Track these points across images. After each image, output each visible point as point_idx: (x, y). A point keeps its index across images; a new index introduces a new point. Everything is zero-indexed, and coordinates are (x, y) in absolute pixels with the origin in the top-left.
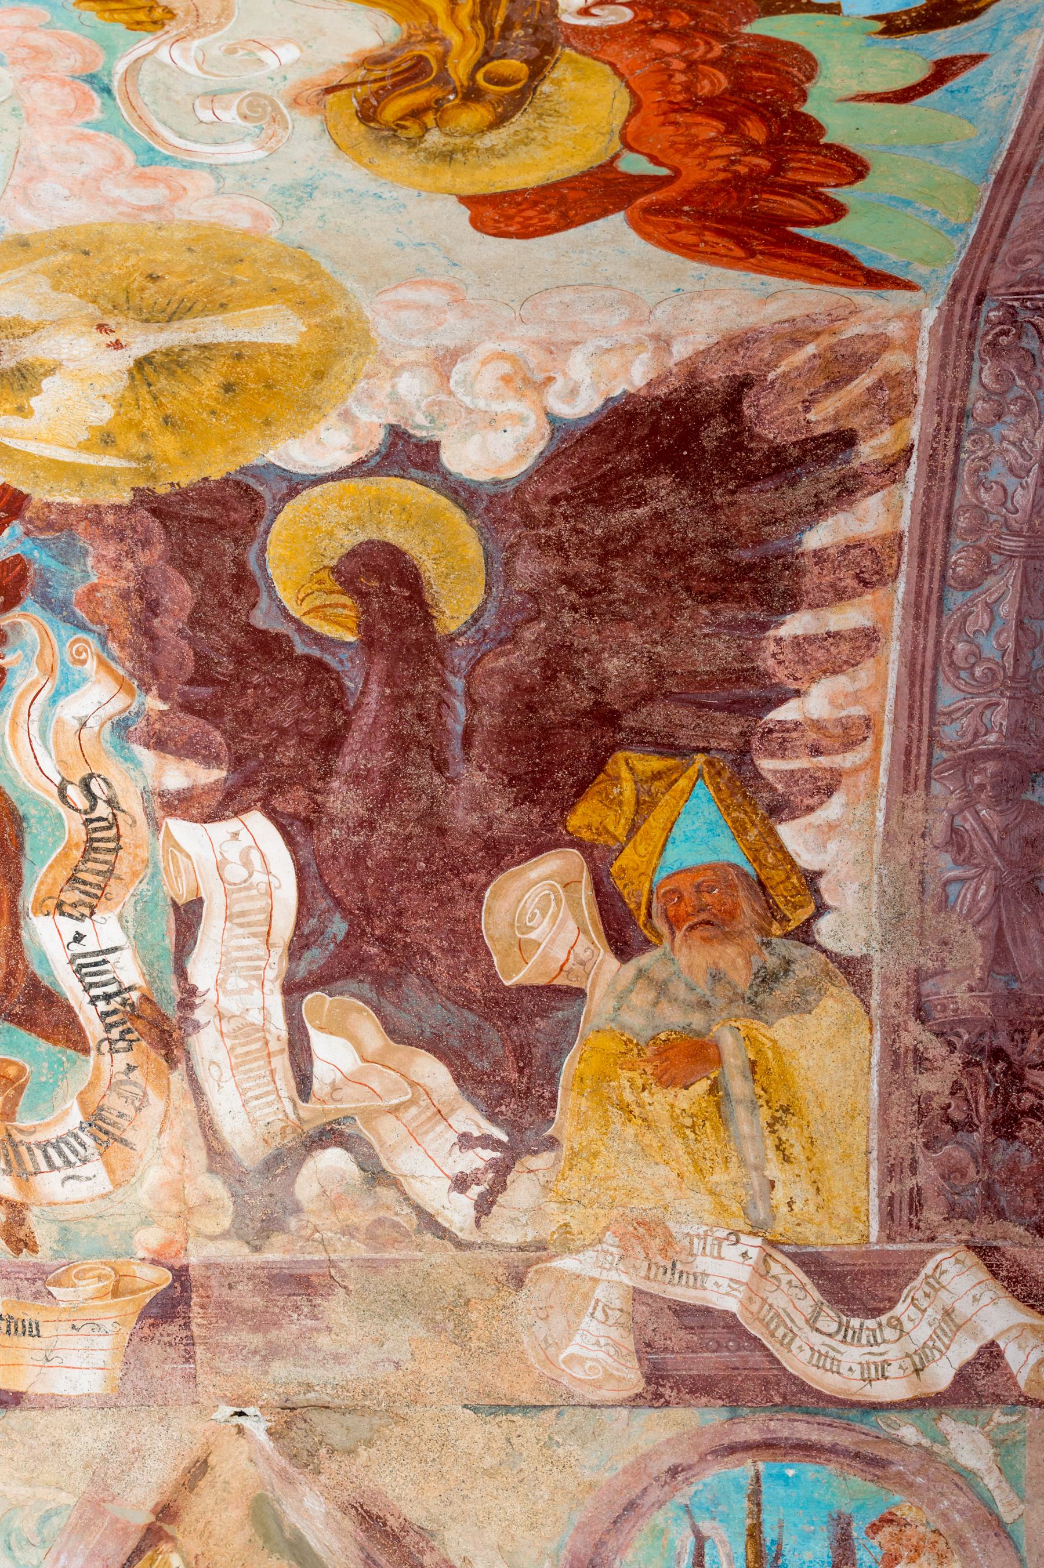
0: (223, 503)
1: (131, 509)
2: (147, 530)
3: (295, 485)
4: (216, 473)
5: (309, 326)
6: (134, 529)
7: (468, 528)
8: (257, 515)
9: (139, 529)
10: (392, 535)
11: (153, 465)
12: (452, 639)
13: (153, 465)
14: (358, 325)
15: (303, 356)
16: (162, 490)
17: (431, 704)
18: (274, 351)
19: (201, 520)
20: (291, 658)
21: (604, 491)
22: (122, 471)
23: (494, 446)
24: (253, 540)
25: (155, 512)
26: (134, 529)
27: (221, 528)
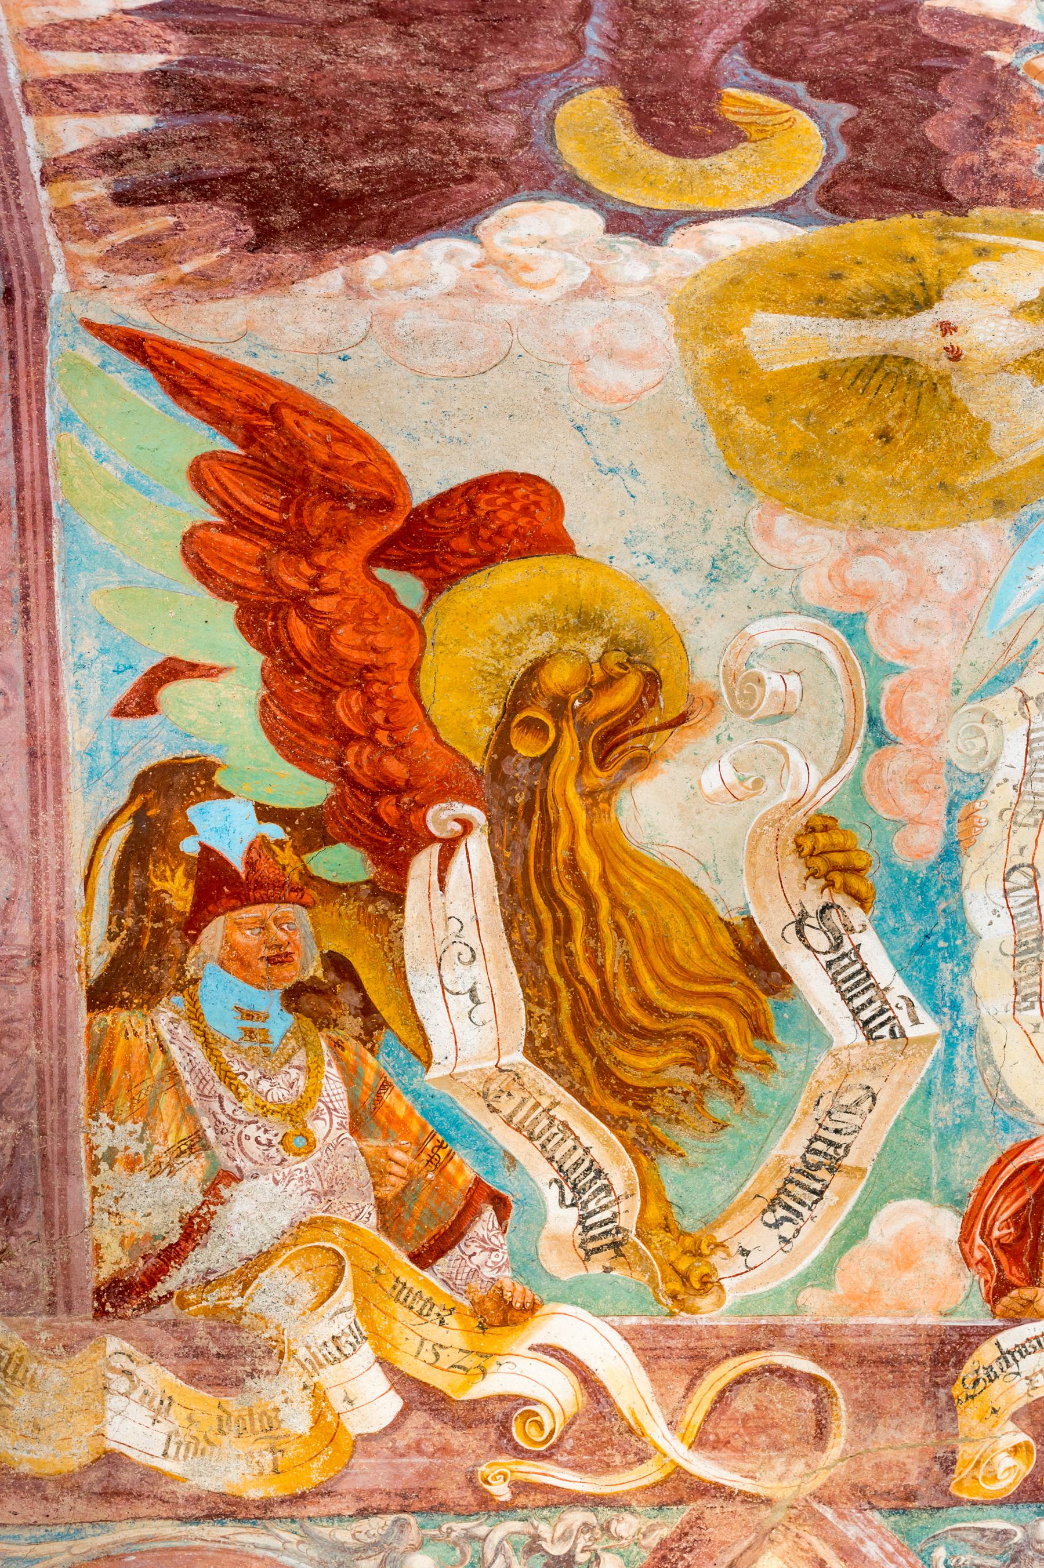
0: (864, 199)
1: (975, 202)
2: (961, 182)
3: (780, 210)
4: (869, 223)
5: (739, 334)
6: (977, 183)
7: (574, 164)
8: (827, 188)
9: (970, 184)
10: (670, 163)
11: (939, 232)
12: (601, 83)
13: (939, 232)
14: (686, 331)
15: (750, 298)
16: (935, 214)
17: (631, 40)
18: (781, 306)
19: (895, 187)
20: (812, 81)
21: (408, 182)
22: (976, 230)
23: (539, 234)
24: (838, 167)
25: (949, 197)
26: (977, 183)
27: (873, 179)
